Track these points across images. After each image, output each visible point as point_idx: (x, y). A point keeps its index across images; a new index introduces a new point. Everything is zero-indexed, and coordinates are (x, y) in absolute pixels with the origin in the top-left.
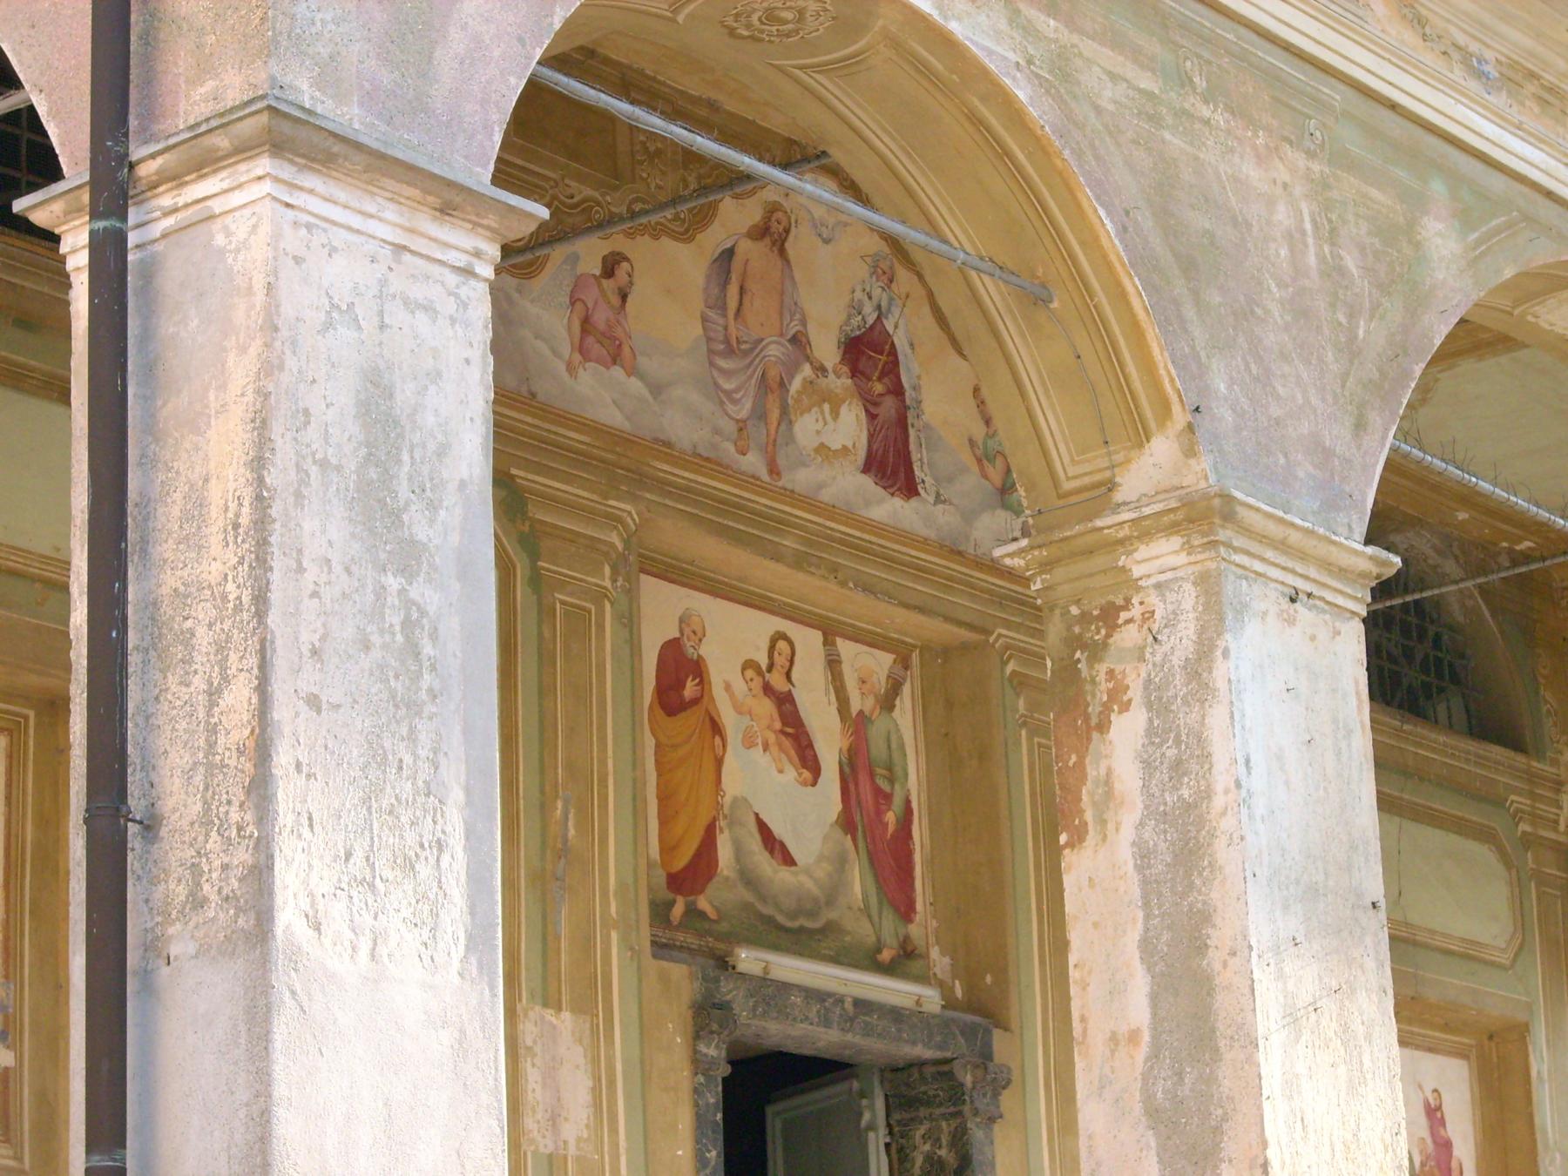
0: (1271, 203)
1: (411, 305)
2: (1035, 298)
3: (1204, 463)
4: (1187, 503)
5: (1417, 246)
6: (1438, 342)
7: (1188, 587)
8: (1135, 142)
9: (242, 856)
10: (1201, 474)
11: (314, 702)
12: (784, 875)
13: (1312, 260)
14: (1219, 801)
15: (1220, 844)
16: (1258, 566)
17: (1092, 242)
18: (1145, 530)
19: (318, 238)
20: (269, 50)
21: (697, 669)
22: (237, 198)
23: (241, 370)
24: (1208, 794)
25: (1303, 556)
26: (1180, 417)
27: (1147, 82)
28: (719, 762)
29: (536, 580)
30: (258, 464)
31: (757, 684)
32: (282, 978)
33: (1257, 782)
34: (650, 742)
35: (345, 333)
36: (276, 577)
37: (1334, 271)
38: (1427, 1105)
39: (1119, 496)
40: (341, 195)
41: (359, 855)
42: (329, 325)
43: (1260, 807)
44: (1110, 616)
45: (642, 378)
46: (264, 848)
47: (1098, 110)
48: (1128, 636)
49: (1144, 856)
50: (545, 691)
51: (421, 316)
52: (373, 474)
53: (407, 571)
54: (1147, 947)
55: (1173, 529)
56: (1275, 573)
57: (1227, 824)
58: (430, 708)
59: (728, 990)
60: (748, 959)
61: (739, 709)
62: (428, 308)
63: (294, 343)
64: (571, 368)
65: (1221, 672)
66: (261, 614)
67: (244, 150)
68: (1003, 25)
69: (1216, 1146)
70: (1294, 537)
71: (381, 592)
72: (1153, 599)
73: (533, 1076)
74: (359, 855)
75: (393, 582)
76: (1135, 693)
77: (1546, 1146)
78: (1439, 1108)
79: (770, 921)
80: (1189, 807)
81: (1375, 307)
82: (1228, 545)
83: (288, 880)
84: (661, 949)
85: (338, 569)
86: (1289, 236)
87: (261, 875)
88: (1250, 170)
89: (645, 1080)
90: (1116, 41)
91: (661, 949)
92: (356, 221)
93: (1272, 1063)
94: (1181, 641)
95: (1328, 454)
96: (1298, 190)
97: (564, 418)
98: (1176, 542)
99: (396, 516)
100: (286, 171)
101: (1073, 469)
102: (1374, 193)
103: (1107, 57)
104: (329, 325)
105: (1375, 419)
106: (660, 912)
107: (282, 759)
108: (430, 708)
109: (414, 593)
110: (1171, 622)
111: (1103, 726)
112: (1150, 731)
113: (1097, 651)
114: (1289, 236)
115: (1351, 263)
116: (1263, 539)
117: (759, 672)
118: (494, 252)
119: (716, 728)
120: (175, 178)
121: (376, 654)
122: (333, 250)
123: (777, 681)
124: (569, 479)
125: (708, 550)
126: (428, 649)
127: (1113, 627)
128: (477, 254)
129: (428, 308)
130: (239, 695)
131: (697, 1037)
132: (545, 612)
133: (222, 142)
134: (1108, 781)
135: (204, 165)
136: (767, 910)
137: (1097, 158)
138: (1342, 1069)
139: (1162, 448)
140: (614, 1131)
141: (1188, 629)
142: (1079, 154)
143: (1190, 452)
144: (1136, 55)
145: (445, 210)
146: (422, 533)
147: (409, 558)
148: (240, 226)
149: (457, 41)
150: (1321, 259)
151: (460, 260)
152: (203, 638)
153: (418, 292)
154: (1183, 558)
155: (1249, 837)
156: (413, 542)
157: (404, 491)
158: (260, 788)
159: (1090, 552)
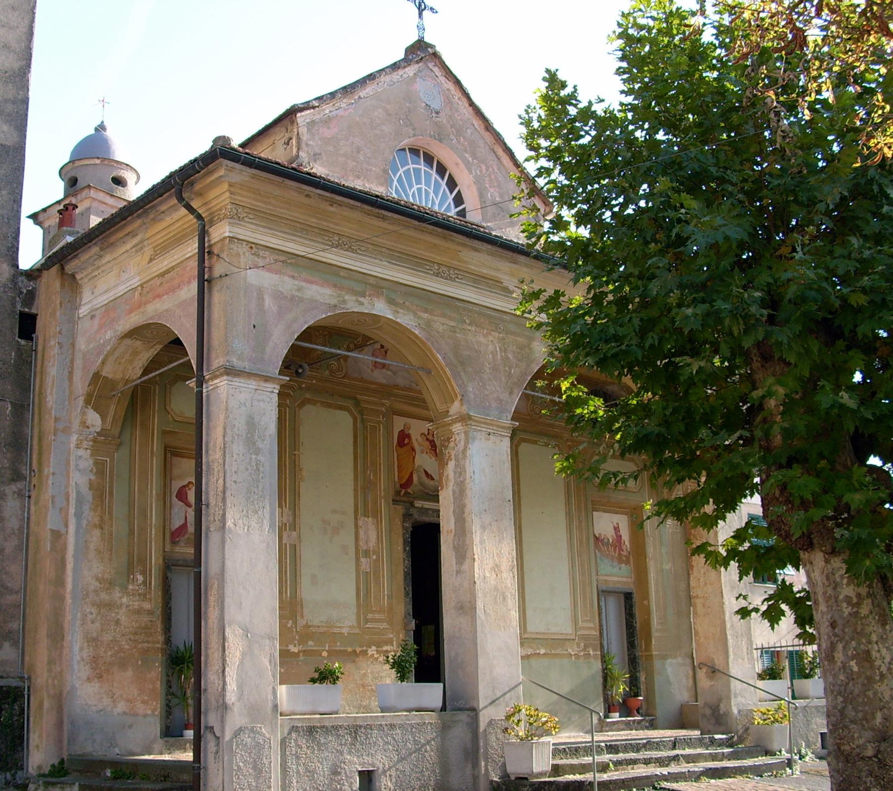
0: (487, 346)
1: (258, 401)
2: (429, 372)
3: (465, 407)
4: (461, 416)
5: (531, 349)
6: (535, 371)
7: (463, 434)
8: (449, 338)
9: (221, 512)
10: (464, 409)
11: (235, 482)
12: (432, 482)
13: (499, 357)
14: (467, 481)
15: (467, 490)
16: (479, 428)
17: (437, 360)
18: (454, 421)
19: (237, 390)
20: (227, 354)
21: (409, 436)
22: (222, 384)
23: (222, 417)
24: (465, 480)
25: (492, 425)
26: (459, 397)
27: (453, 324)
28: (414, 457)
29: (362, 421)
30: (224, 436)
31: (425, 438)
32: (228, 536)
33: (476, 476)
34: (396, 455)
35: (243, 408)
36: (227, 458)
37: (505, 359)
38: (614, 527)
39: (450, 414)
40: (243, 381)
41: (245, 512)
42: (240, 407)
43: (477, 481)
44: (449, 439)
45: (391, 371)
46: (224, 510)
47: (438, 332)
48: (452, 444)
49: (454, 492)
50: (365, 445)
51: (261, 403)
52: (249, 435)
53: (257, 454)
54: (454, 511)
55: (459, 421)
56: (484, 429)
57: (468, 486)
58: (262, 481)
59: (412, 511)
60: (418, 504)
61: (419, 444)
62: (263, 401)
63: (232, 412)
64: (372, 371)
65: (469, 452)
66: (224, 466)
67: (222, 375)
68: (412, 318)
69: (465, 555)
70: (488, 421)
71: (251, 459)
72: (456, 436)
73: (361, 533)
74: (245, 512)
75: (254, 457)
76: (453, 457)
77: (648, 536)
78: (618, 527)
79: (427, 494)
80: (462, 482)
81: (517, 366)
82: (471, 425)
83: (229, 516)
84: (395, 502)
85: (241, 455)
86: (492, 353)
87: (224, 515)
88: (482, 339)
89: (390, 531)
90: (444, 315)
91: (395, 502)
92: (246, 386)
93: (477, 539)
94: (461, 445)
95: (501, 400)
96: (495, 342)
97: (371, 383)
98: (460, 424)
99: (254, 444)
100: (230, 378)
101: (441, 407)
102: (518, 339)
103: (442, 320)
104: (240, 407)
105: (516, 391)
106: (398, 493)
107: (228, 494)
108: (262, 481)
109: (258, 458)
110: (459, 442)
111: (447, 464)
112: (455, 466)
113: (446, 447)
114: (492, 353)
115: (510, 356)
116: (480, 422)
117: (425, 435)
118: (278, 387)
119: (413, 450)
120: (212, 379)
121: (249, 471)
122: (241, 392)
123: (430, 437)
124: (370, 396)
125: (411, 409)
126: (261, 469)
127: (449, 442)
128: (274, 388)
129: (263, 401)
130: (221, 481)
131: (403, 522)
132: (365, 428)
133: (218, 373)
134: (448, 476)
135: (216, 377)
136: (427, 491)
137: (437, 343)
138: (497, 537)
139: (457, 404)
140: (382, 544)
141: (462, 443)
142: (432, 343)
143: (462, 405)
144: (450, 318)
145: (266, 381)
146: (260, 446)
147: (257, 451)
148: (222, 388)
149: (271, 344)
150: (501, 356)
151: (270, 390)
152: (216, 470)
153: (260, 398)
154: (462, 428)
155: (473, 488)
156: (258, 448)
157: (256, 438)
158: (224, 500)
159: (444, 426)
